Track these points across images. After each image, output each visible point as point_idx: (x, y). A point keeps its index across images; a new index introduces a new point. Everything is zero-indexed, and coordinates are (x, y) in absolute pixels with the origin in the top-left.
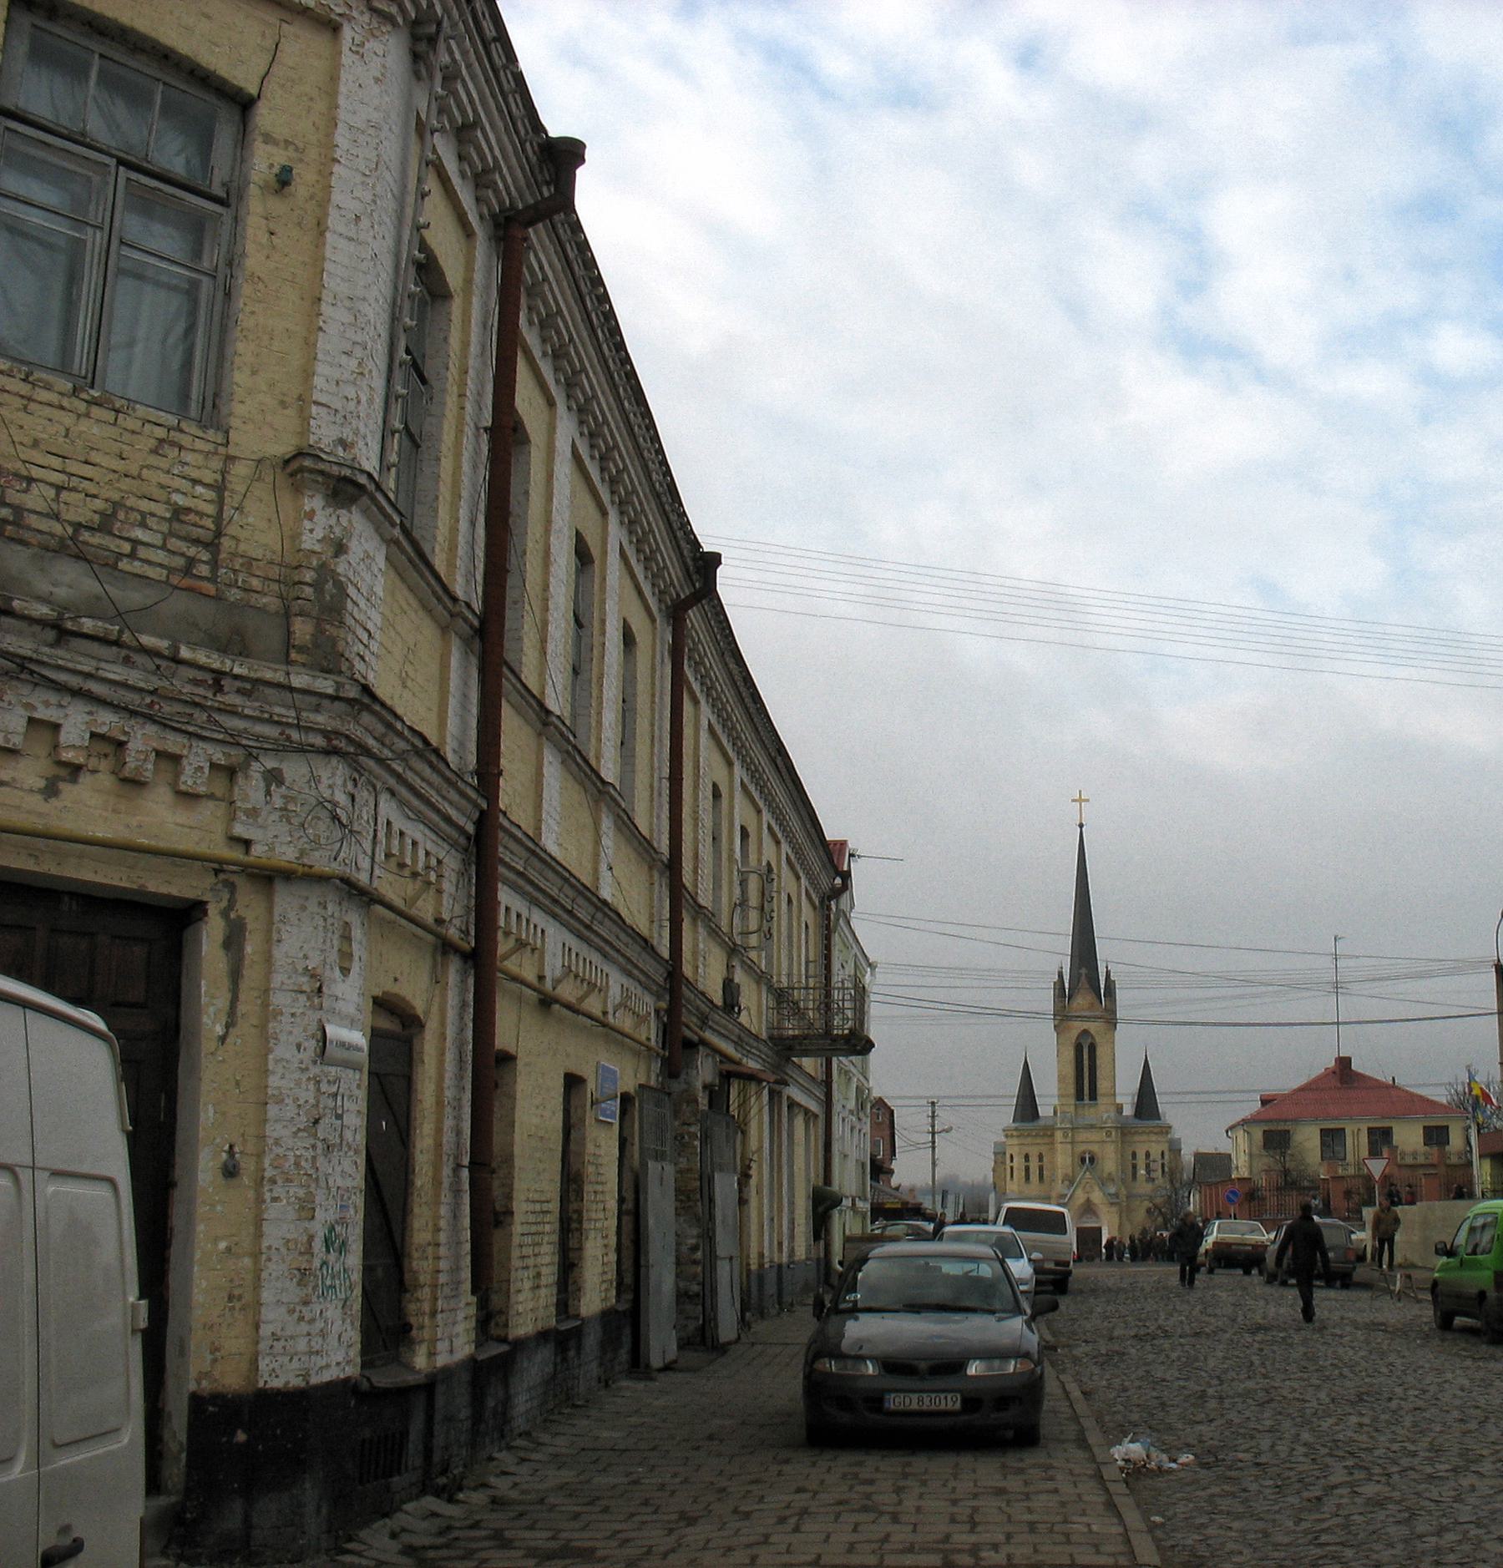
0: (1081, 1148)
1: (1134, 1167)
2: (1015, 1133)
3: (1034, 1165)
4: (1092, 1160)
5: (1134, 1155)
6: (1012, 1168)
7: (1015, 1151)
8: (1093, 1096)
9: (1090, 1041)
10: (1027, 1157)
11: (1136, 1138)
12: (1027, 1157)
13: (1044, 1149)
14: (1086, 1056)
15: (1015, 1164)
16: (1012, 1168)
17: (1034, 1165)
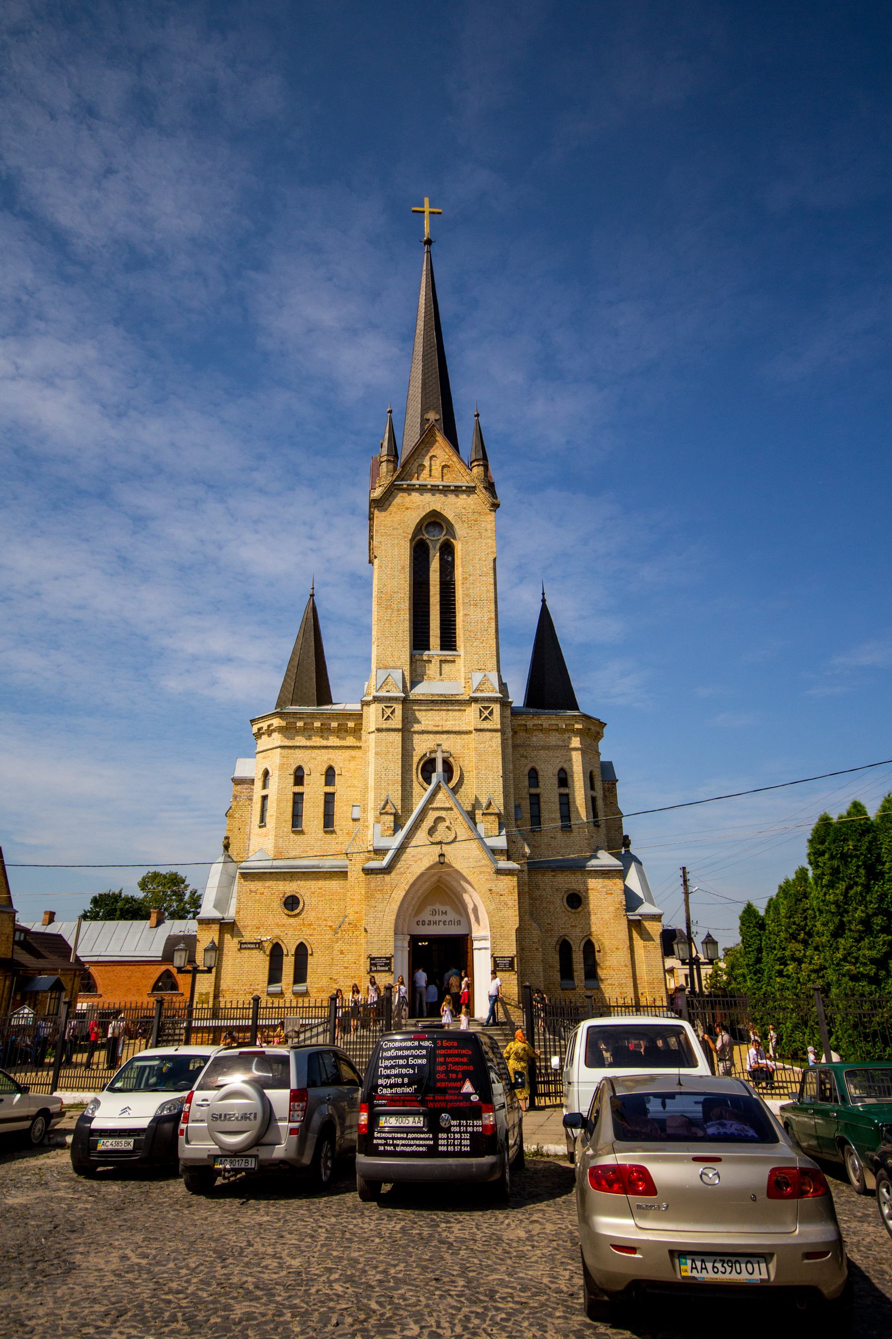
0: (422, 746)
1: (535, 800)
2: (276, 722)
3: (314, 789)
4: (448, 768)
5: (533, 775)
6: (265, 798)
7: (273, 761)
8: (448, 642)
9: (442, 538)
10: (299, 777)
11: (538, 739)
12: (299, 777)
13: (338, 759)
14: (435, 565)
15: (272, 790)
16: (265, 798)
17: (314, 789)
